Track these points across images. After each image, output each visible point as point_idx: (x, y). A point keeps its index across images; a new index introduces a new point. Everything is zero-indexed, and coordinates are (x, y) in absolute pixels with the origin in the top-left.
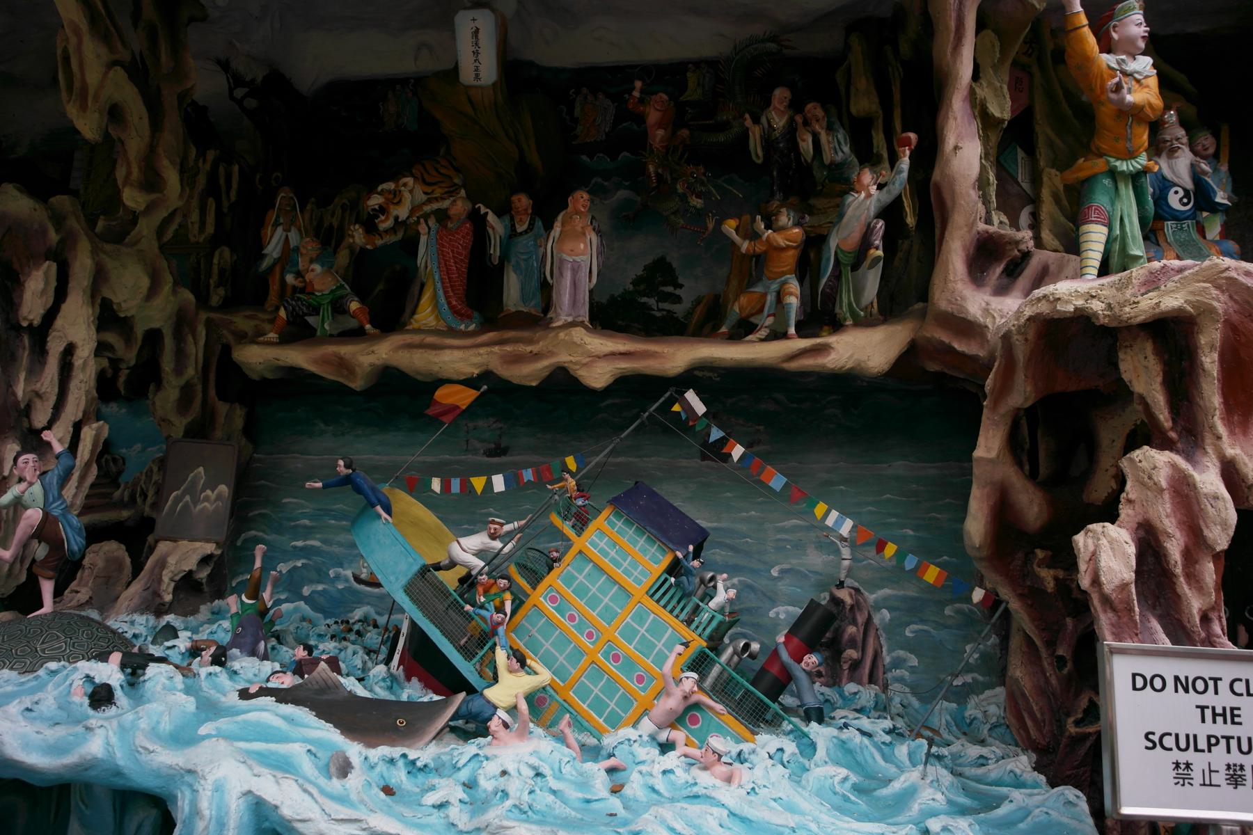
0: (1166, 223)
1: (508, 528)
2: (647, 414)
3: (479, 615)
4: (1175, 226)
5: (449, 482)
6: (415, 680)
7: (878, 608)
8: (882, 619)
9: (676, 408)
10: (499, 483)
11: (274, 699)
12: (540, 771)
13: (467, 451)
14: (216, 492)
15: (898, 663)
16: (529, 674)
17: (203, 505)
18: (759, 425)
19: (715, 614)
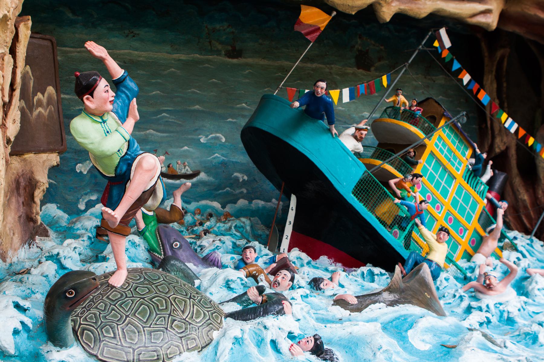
14: (46, 95)
17: (38, 111)
18: (382, 46)
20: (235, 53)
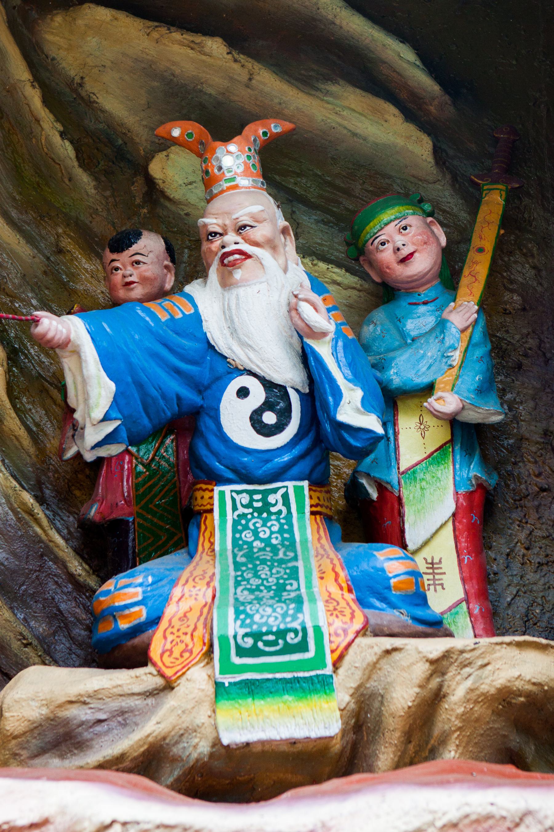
0: (217, 489)
4: (246, 500)
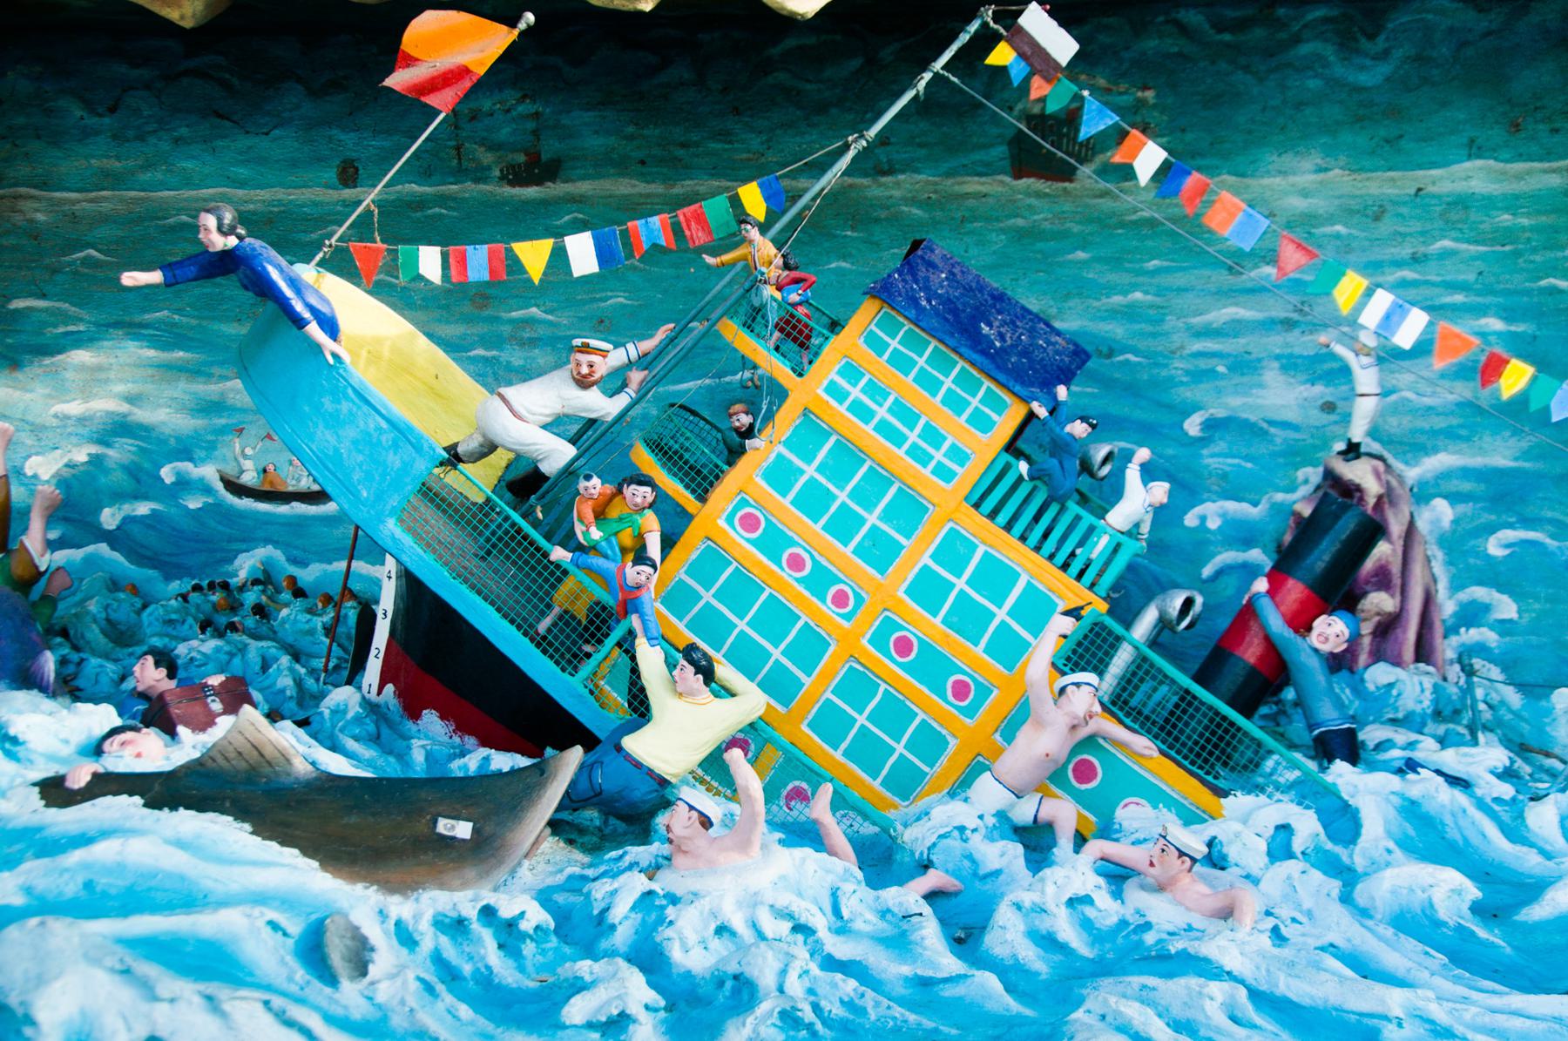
1: (617, 357)
2: (927, 76)
3: (589, 570)
5: (463, 261)
6: (430, 718)
7: (1422, 494)
8: (1436, 522)
9: (1003, 55)
10: (582, 253)
11: (137, 800)
12: (802, 921)
13: (460, 173)
15: (1472, 615)
16: (717, 696)
18: (1145, 88)
19: (1124, 539)
20: (536, 170)
